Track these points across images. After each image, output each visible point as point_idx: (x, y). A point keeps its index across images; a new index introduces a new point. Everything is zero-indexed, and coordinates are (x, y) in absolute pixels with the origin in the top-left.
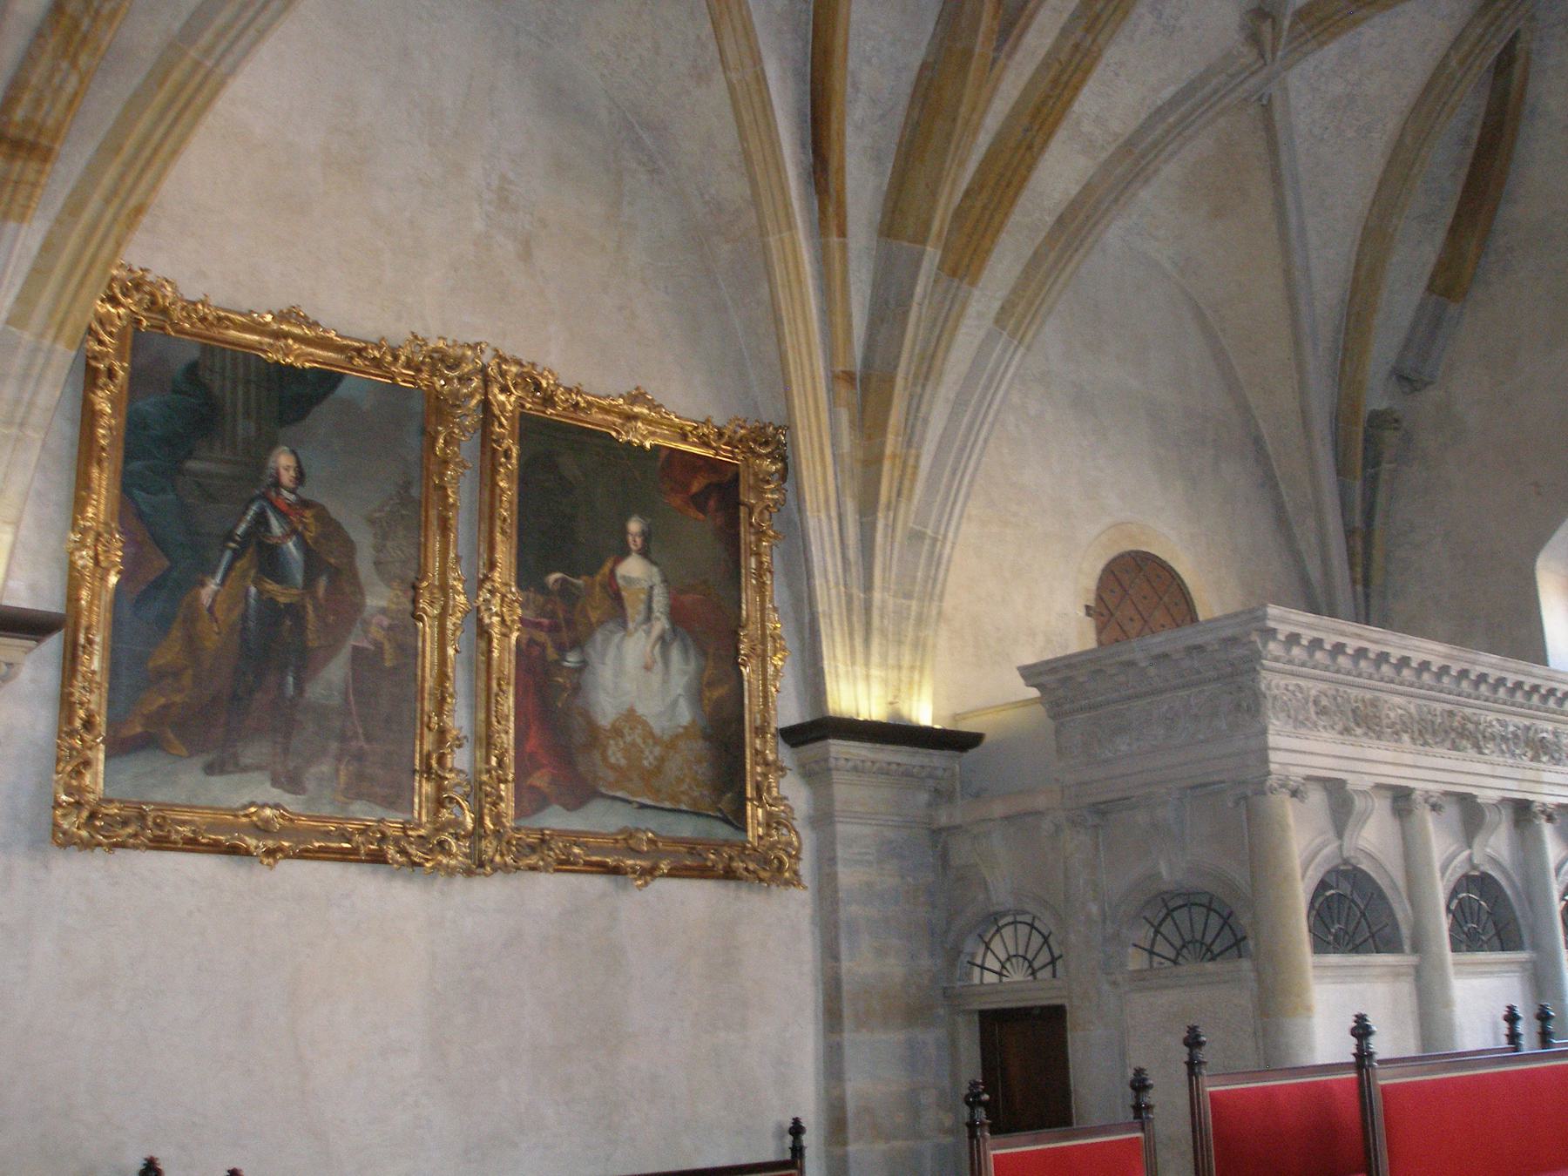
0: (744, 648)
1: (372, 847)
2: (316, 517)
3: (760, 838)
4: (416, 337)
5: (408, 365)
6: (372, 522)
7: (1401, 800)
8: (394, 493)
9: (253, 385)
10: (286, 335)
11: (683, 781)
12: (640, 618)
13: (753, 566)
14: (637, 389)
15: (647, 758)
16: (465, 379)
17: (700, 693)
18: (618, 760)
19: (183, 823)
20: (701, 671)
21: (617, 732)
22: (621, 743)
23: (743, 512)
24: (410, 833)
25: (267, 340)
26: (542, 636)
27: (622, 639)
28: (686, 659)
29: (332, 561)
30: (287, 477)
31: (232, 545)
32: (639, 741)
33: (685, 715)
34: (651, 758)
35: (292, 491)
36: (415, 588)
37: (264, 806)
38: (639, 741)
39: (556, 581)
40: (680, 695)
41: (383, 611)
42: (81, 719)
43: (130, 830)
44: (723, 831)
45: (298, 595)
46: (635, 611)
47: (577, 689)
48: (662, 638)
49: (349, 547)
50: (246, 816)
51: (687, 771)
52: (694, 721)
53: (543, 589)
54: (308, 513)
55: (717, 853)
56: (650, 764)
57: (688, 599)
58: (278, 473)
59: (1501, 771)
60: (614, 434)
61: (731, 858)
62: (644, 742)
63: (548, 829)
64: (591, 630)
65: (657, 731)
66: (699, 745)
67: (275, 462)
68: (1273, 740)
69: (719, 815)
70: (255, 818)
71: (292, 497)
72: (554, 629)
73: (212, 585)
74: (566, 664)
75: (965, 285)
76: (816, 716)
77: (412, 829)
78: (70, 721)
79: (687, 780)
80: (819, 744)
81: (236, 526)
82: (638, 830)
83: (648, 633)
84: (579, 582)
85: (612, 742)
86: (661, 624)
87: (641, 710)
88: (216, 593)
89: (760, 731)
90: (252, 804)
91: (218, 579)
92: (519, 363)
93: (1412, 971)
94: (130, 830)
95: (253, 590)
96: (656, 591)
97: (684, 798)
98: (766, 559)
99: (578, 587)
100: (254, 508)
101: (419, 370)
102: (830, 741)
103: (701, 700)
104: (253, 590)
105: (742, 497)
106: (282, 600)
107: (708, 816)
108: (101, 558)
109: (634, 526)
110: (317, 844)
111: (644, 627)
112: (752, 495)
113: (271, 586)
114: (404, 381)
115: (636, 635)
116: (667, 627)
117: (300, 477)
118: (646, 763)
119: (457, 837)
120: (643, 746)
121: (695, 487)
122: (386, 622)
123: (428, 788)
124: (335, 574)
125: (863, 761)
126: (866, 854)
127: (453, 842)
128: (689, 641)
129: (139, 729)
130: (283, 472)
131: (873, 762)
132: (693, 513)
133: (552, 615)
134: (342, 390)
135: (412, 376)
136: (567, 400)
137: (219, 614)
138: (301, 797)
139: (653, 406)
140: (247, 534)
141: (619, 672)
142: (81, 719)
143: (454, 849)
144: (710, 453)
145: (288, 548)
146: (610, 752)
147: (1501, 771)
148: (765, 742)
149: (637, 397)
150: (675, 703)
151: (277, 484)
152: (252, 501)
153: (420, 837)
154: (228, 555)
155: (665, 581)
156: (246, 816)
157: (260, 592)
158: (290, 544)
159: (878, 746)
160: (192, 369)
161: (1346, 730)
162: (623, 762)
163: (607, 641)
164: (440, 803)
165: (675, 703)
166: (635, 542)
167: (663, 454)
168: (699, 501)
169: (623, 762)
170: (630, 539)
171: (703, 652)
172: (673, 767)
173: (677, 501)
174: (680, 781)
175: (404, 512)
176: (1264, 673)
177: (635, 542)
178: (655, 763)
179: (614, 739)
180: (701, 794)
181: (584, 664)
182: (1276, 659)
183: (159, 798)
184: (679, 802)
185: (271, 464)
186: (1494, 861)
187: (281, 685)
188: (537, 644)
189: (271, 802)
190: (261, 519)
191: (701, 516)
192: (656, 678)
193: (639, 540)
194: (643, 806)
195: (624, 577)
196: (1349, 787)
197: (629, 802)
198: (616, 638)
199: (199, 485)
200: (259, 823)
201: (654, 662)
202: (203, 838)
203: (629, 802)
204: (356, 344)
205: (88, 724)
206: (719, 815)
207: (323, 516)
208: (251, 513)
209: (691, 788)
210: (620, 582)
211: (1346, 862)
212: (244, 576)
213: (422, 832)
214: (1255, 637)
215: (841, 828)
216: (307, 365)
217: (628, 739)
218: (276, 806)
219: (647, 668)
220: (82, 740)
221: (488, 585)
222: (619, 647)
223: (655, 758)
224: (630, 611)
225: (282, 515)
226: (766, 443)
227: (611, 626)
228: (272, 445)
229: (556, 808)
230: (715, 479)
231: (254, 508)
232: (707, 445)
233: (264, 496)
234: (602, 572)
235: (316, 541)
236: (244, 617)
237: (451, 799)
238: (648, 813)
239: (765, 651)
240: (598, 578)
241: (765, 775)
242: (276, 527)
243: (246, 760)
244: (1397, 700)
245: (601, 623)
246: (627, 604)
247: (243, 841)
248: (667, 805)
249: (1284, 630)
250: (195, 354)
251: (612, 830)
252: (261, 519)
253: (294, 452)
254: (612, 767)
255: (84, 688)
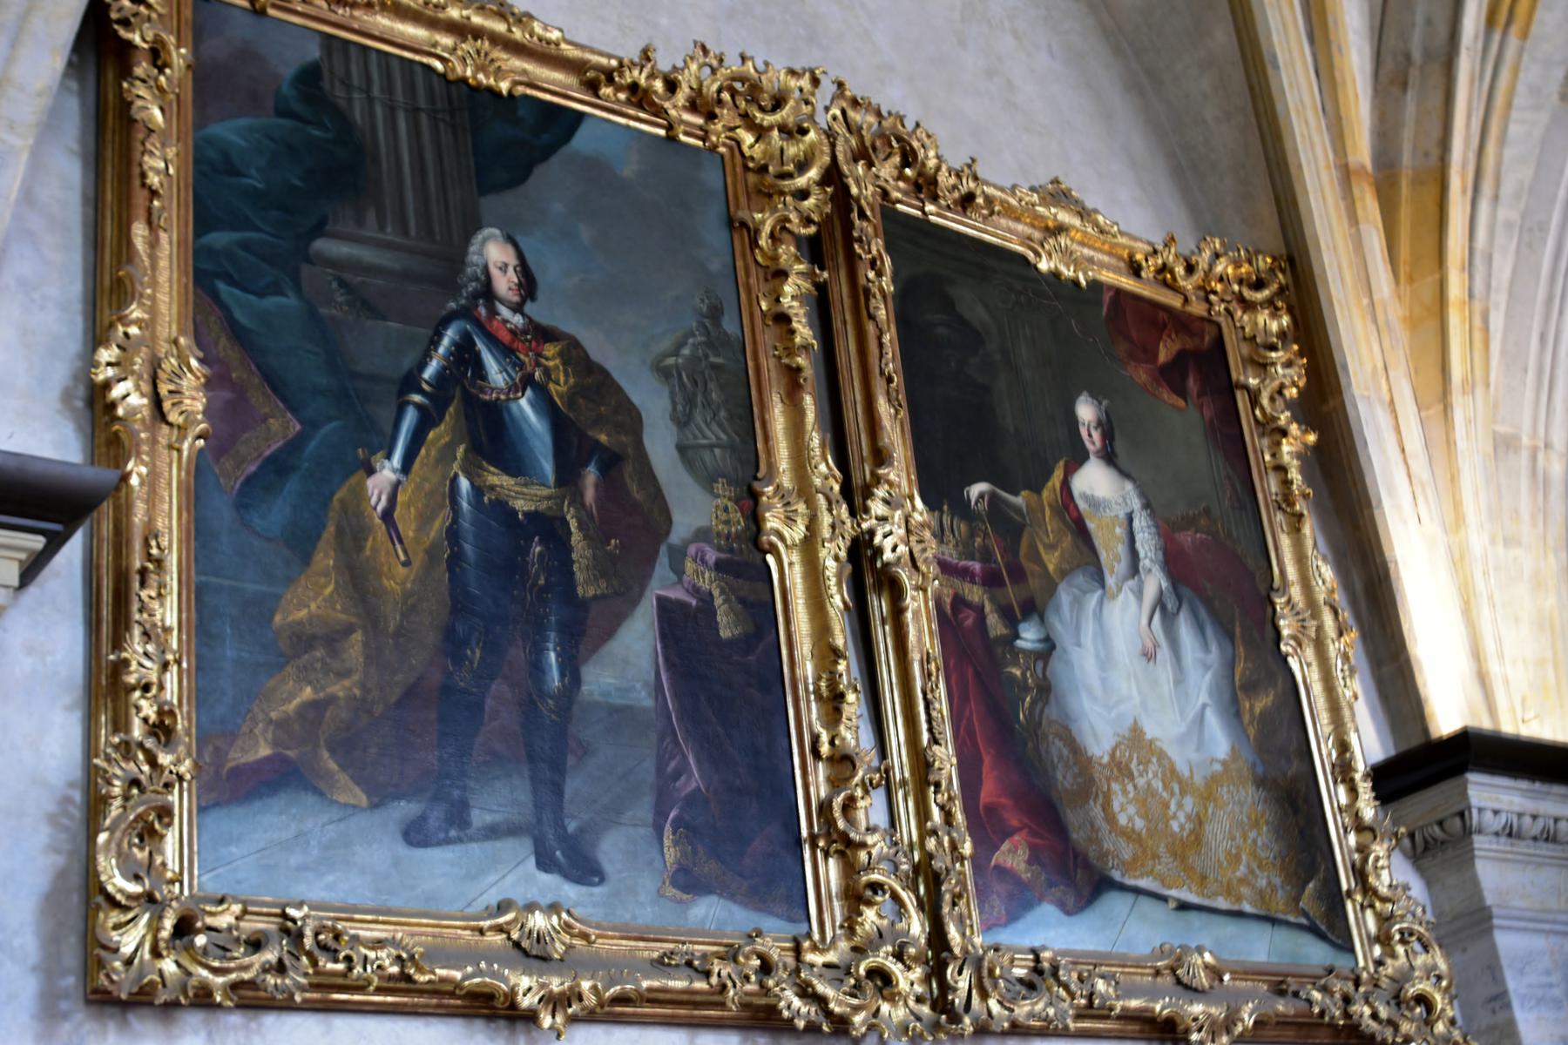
0: (1286, 627)
1: (748, 987)
2: (563, 355)
3: (1379, 963)
4: (705, 51)
5: (693, 106)
6: (664, 373)
8: (694, 324)
9: (424, 118)
10: (478, 33)
11: (1237, 858)
12: (1122, 567)
13: (1274, 489)
14: (1056, 181)
15: (1175, 817)
16: (794, 132)
17: (1235, 701)
18: (1130, 819)
19: (378, 944)
20: (1230, 665)
21: (1121, 769)
22: (1130, 787)
23: (1242, 400)
24: (810, 957)
25: (447, 40)
26: (975, 593)
27: (1101, 603)
28: (1206, 647)
29: (603, 438)
30: (505, 284)
31: (417, 398)
32: (1158, 785)
33: (1220, 742)
34: (1182, 820)
35: (517, 308)
36: (755, 496)
37: (531, 907)
38: (1158, 785)
39: (981, 496)
40: (1204, 706)
41: (702, 535)
42: (145, 720)
43: (270, 956)
44: (1316, 953)
45: (549, 498)
46: (1111, 553)
47: (1045, 690)
48: (1160, 603)
49: (630, 421)
50: (500, 929)
51: (1239, 841)
52: (1233, 749)
53: (962, 508)
54: (550, 350)
55: (1325, 990)
56: (1182, 827)
57: (1186, 538)
58: (486, 269)
60: (1031, 256)
61: (1347, 1000)
62: (1165, 787)
63: (1044, 948)
64: (1051, 588)
65: (1182, 768)
66: (1249, 794)
67: (480, 253)
69: (1303, 921)
70: (515, 936)
71: (518, 320)
72: (991, 580)
73: (387, 472)
74: (1019, 643)
75: (1513, 42)
76: (1416, 741)
77: (814, 948)
78: (120, 724)
79: (1244, 857)
80: (1446, 788)
81: (422, 366)
82: (1186, 949)
83: (1139, 593)
84: (1019, 500)
85: (1115, 787)
86: (1155, 581)
87: (1151, 731)
88: (396, 486)
89: (1344, 770)
90: (503, 907)
91: (397, 459)
92: (879, 114)
94: (270, 956)
95: (464, 484)
96: (1136, 524)
97: (1245, 890)
98: (1295, 475)
99: (1018, 510)
100: (449, 336)
101: (711, 117)
102: (1473, 777)
103: (1238, 714)
104: (464, 484)
105: (1234, 376)
106: (521, 505)
107: (1287, 924)
108: (167, 405)
109: (1086, 411)
110: (645, 984)
111: (1131, 583)
112: (1250, 371)
113: (496, 478)
114: (687, 134)
115: (1121, 597)
116: (1164, 584)
117: (528, 285)
118: (1175, 826)
119: (899, 956)
120: (1165, 794)
121: (1164, 355)
122: (712, 556)
123: (832, 871)
124: (611, 463)
125: (1520, 815)
126: (1551, 985)
127: (896, 968)
128: (1203, 613)
129: (264, 751)
130: (495, 272)
131: (1535, 817)
132: (1166, 395)
133: (986, 556)
134: (582, 140)
135: (701, 128)
136: (955, 187)
137: (408, 529)
138: (597, 890)
139: (1084, 213)
140: (441, 378)
141: (1106, 662)
142: (145, 720)
143: (903, 985)
144: (1175, 302)
145: (520, 409)
146: (1116, 806)
148: (1353, 791)
149: (1058, 195)
150: (1201, 717)
151: (487, 292)
152: (445, 322)
153: (827, 966)
154: (410, 418)
155: (1147, 506)
156: (500, 929)
157: (478, 490)
158: (523, 402)
159: (1537, 785)
160: (310, 76)
162: (1139, 824)
163: (1078, 603)
164: (855, 898)
165: (1201, 717)
166: (1093, 440)
167: (1107, 297)
168: (1172, 375)
169: (1139, 824)
170: (1084, 432)
171: (1227, 633)
172: (1219, 834)
173: (1141, 375)
174: (1235, 859)
175: (713, 359)
177: (1093, 440)
178: (1188, 826)
179: (1116, 780)
180: (1269, 883)
181: (1049, 646)
183: (318, 894)
184: (1239, 899)
185: (474, 258)
187: (537, 668)
188: (968, 605)
189: (545, 901)
190: (465, 355)
191: (1181, 403)
192: (1164, 670)
193: (1096, 435)
194: (1183, 906)
195: (1085, 497)
197: (1164, 899)
198: (1093, 600)
199: (343, 283)
200: (525, 944)
201: (1156, 646)
202: (420, 970)
203: (1164, 899)
204: (603, 61)
205: (162, 729)
206: (1303, 921)
207: (574, 354)
208: (446, 342)
209: (1252, 872)
210: (1082, 505)
212: (446, 455)
213: (831, 957)
215: (1506, 942)
216: (520, 89)
217: (1141, 782)
218: (554, 908)
219: (1149, 656)
220: (152, 761)
221: (881, 492)
222: (1099, 614)
223: (1188, 817)
224: (1103, 556)
225: (506, 352)
226: (1259, 285)
227: (1080, 579)
228: (472, 225)
229: (1048, 910)
230: (1190, 344)
231: (449, 336)
232: (1172, 286)
233: (466, 313)
234: (1050, 484)
235: (571, 397)
236: (453, 534)
237: (876, 887)
238: (1194, 918)
239: (1320, 629)
240: (1045, 494)
241: (1363, 849)
242: (496, 373)
243: (480, 817)
245: (1064, 574)
246: (1098, 542)
247: (505, 980)
248: (1222, 903)
250: (314, 52)
251: (1142, 949)
252: (465, 355)
253: (511, 240)
254: (1129, 835)
255: (146, 654)
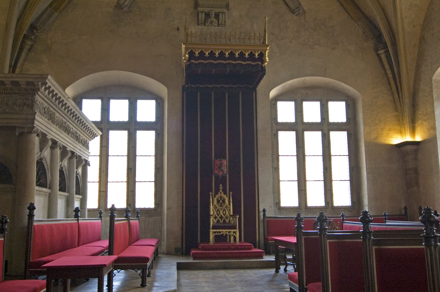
7: (55, 143)
59: (71, 142)
68: (37, 117)
93: (48, 194)
147: (71, 142)
161: (48, 120)
176: (37, 96)
182: (42, 93)
186: (65, 166)
196: (47, 137)
211: (41, 159)
214: (40, 84)
244: (57, 115)
249: (49, 84)
